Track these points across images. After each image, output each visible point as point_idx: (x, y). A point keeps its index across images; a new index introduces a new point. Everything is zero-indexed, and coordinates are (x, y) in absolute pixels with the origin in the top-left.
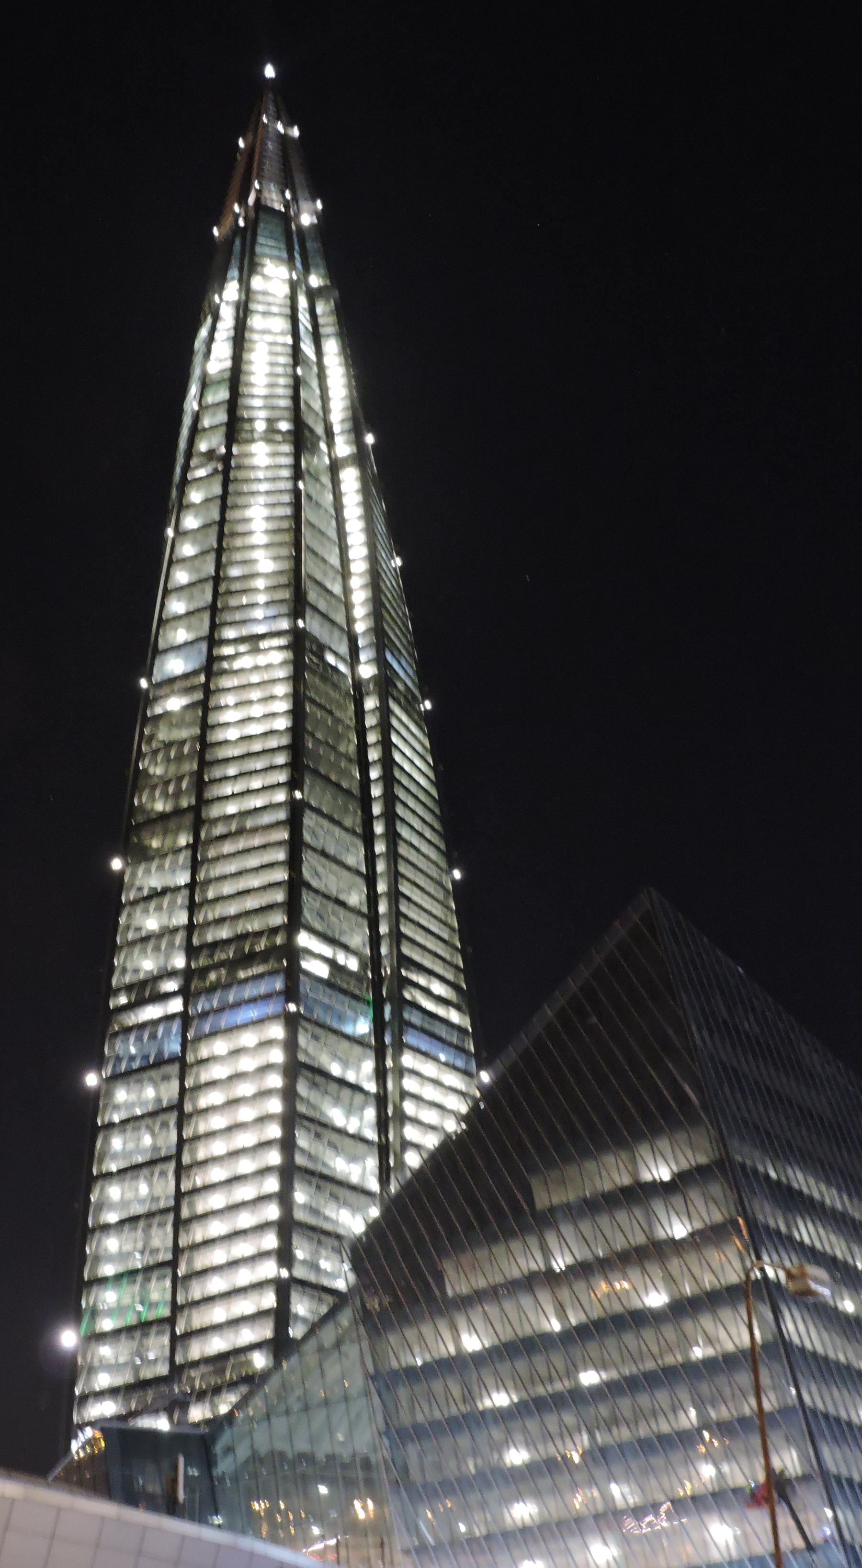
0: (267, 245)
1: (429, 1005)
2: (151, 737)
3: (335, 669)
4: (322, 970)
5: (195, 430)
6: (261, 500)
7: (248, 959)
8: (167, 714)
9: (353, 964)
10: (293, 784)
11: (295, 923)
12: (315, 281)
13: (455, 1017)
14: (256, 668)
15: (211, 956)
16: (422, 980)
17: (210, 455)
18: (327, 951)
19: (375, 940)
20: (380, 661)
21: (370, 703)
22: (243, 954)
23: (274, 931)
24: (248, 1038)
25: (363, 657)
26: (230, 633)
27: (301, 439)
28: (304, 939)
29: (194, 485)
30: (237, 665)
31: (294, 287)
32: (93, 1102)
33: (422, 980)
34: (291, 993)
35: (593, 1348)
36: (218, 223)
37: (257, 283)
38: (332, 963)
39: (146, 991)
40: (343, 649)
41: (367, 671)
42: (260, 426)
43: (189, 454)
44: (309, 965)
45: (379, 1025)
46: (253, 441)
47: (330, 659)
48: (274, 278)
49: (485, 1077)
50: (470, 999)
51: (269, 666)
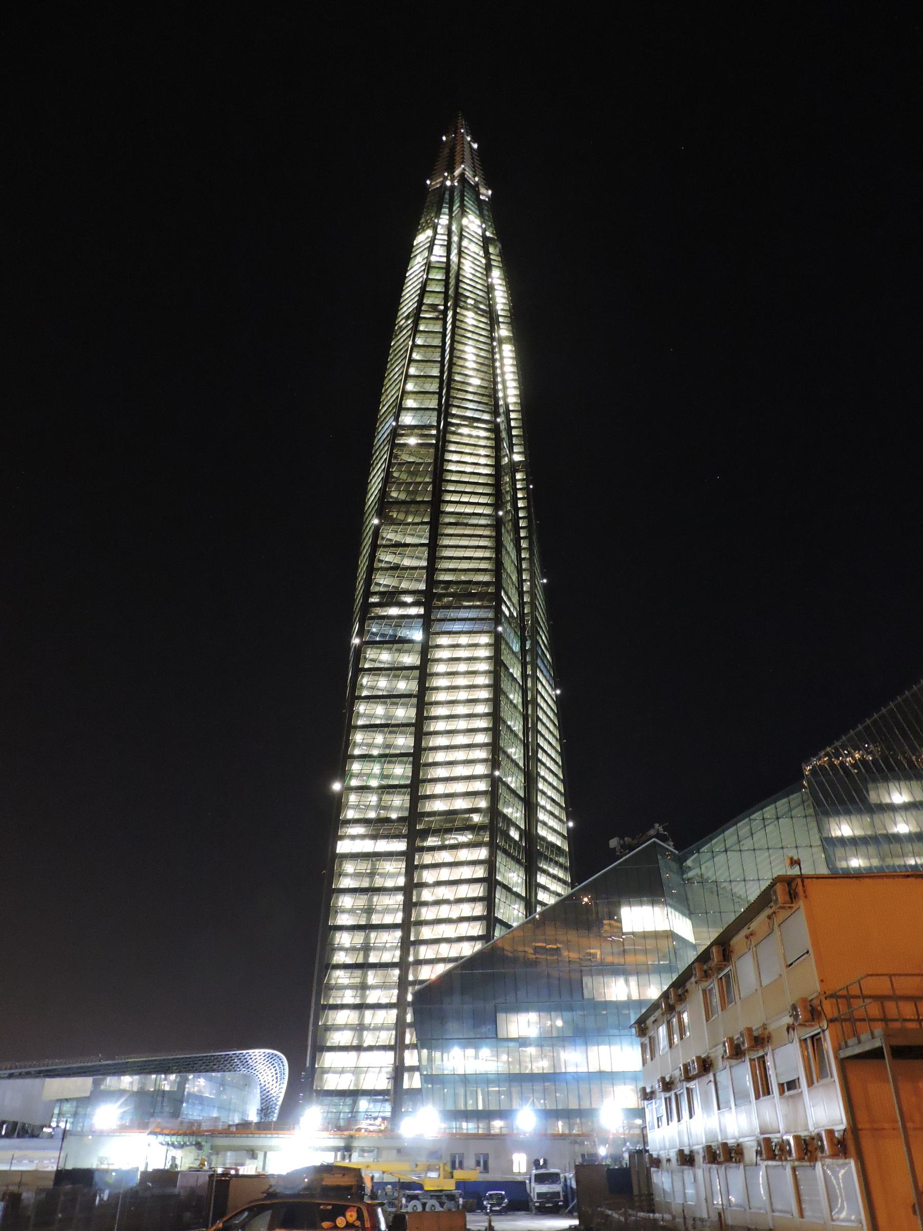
0: (469, 203)
2: (396, 457)
4: (507, 613)
5: (423, 292)
6: (470, 342)
7: (471, 596)
8: (405, 445)
10: (497, 506)
12: (488, 234)
14: (470, 436)
15: (446, 589)
17: (434, 307)
19: (522, 604)
22: (464, 593)
23: (487, 584)
24: (464, 640)
29: (423, 321)
30: (460, 431)
35: (863, 849)
36: (431, 180)
37: (465, 221)
39: (391, 597)
43: (420, 303)
44: (504, 608)
46: (467, 309)
48: (473, 223)
51: (478, 437)
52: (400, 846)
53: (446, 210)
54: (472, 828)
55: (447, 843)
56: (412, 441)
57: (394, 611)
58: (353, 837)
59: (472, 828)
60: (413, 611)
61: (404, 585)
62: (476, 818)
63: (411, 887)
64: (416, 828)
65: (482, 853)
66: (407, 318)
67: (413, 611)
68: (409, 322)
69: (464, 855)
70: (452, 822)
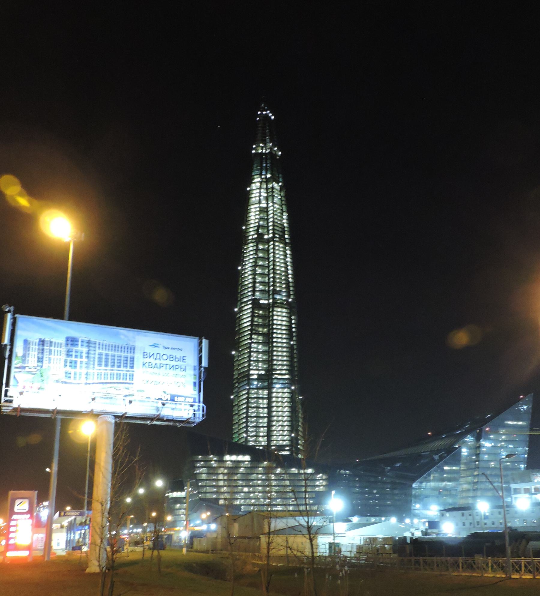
1: (279, 377)
3: (263, 304)
9: (263, 372)
11: (250, 370)
12: (269, 176)
13: (287, 377)
16: (278, 372)
18: (256, 372)
20: (274, 299)
21: (271, 310)
25: (271, 297)
26: (245, 300)
27: (260, 239)
28: (252, 372)
31: (261, 182)
32: (232, 401)
33: (278, 372)
34: (249, 384)
38: (258, 374)
40: (267, 296)
41: (271, 301)
42: (250, 237)
45: (268, 383)
47: (261, 302)
49: (293, 388)
50: (291, 372)
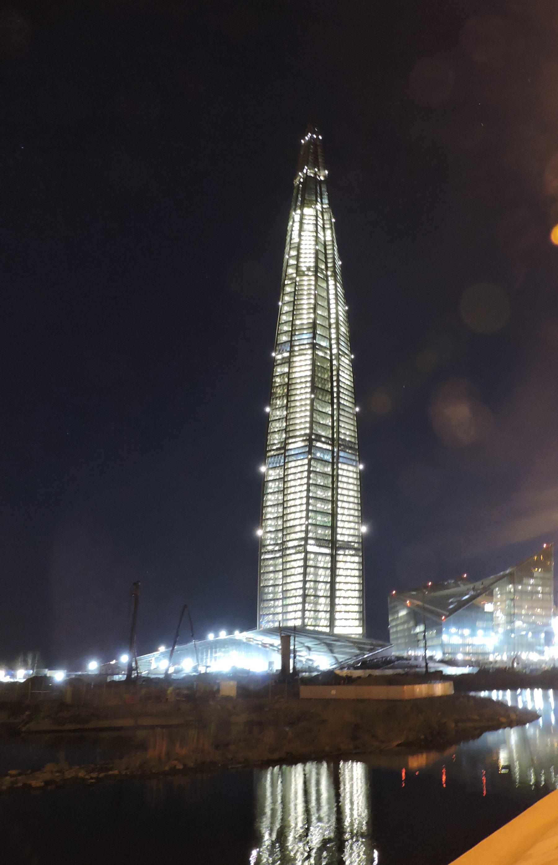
7: (351, 448)
22: (347, 446)
24: (345, 467)
52: (328, 551)
53: (319, 200)
54: (355, 549)
55: (347, 553)
56: (321, 354)
57: (319, 444)
58: (311, 545)
59: (355, 549)
60: (325, 446)
61: (323, 434)
62: (356, 545)
63: (333, 569)
64: (333, 544)
65: (357, 559)
66: (309, 269)
67: (325, 446)
68: (310, 273)
69: (349, 559)
70: (347, 546)
